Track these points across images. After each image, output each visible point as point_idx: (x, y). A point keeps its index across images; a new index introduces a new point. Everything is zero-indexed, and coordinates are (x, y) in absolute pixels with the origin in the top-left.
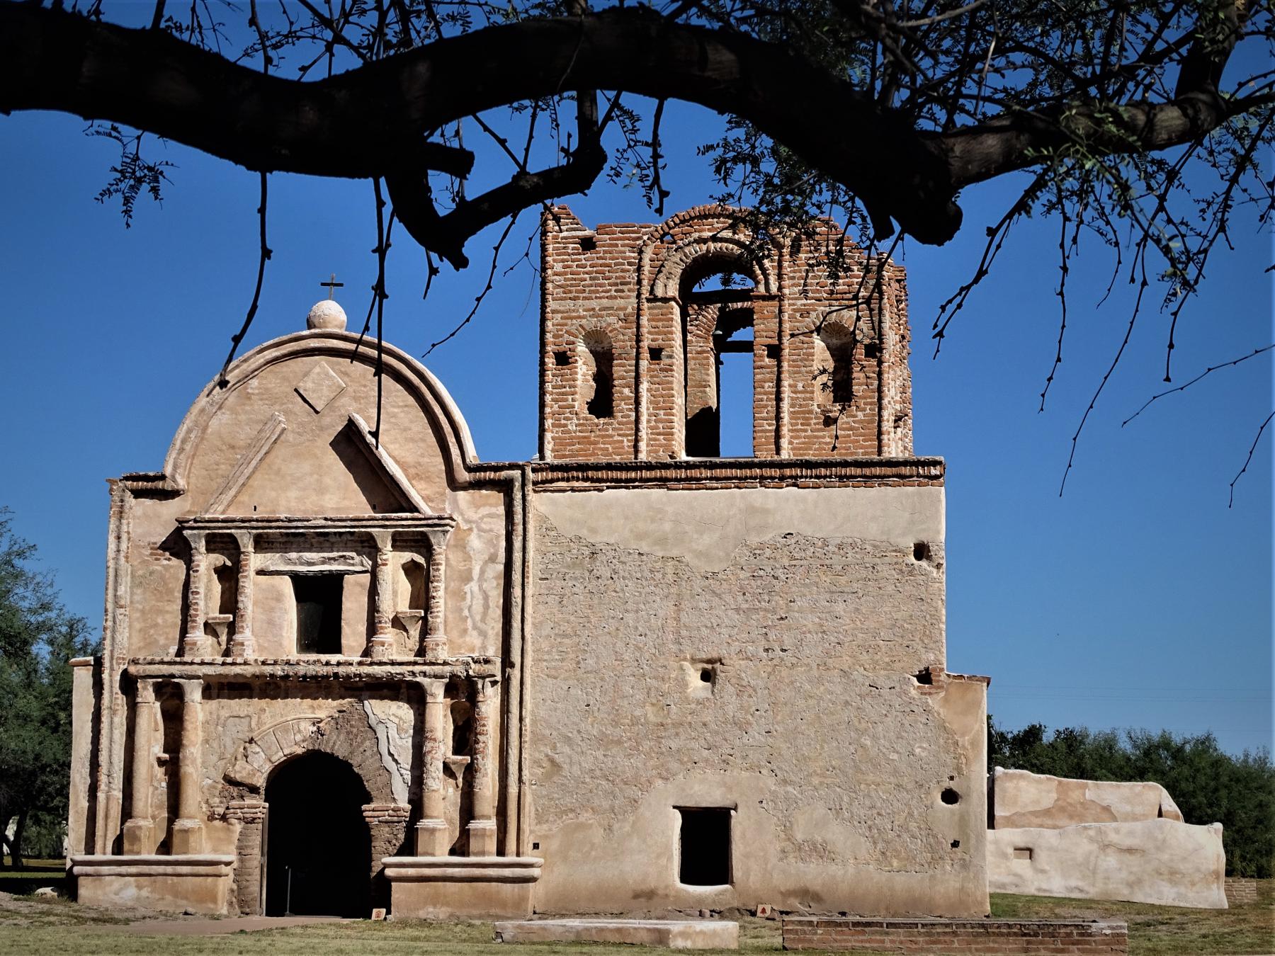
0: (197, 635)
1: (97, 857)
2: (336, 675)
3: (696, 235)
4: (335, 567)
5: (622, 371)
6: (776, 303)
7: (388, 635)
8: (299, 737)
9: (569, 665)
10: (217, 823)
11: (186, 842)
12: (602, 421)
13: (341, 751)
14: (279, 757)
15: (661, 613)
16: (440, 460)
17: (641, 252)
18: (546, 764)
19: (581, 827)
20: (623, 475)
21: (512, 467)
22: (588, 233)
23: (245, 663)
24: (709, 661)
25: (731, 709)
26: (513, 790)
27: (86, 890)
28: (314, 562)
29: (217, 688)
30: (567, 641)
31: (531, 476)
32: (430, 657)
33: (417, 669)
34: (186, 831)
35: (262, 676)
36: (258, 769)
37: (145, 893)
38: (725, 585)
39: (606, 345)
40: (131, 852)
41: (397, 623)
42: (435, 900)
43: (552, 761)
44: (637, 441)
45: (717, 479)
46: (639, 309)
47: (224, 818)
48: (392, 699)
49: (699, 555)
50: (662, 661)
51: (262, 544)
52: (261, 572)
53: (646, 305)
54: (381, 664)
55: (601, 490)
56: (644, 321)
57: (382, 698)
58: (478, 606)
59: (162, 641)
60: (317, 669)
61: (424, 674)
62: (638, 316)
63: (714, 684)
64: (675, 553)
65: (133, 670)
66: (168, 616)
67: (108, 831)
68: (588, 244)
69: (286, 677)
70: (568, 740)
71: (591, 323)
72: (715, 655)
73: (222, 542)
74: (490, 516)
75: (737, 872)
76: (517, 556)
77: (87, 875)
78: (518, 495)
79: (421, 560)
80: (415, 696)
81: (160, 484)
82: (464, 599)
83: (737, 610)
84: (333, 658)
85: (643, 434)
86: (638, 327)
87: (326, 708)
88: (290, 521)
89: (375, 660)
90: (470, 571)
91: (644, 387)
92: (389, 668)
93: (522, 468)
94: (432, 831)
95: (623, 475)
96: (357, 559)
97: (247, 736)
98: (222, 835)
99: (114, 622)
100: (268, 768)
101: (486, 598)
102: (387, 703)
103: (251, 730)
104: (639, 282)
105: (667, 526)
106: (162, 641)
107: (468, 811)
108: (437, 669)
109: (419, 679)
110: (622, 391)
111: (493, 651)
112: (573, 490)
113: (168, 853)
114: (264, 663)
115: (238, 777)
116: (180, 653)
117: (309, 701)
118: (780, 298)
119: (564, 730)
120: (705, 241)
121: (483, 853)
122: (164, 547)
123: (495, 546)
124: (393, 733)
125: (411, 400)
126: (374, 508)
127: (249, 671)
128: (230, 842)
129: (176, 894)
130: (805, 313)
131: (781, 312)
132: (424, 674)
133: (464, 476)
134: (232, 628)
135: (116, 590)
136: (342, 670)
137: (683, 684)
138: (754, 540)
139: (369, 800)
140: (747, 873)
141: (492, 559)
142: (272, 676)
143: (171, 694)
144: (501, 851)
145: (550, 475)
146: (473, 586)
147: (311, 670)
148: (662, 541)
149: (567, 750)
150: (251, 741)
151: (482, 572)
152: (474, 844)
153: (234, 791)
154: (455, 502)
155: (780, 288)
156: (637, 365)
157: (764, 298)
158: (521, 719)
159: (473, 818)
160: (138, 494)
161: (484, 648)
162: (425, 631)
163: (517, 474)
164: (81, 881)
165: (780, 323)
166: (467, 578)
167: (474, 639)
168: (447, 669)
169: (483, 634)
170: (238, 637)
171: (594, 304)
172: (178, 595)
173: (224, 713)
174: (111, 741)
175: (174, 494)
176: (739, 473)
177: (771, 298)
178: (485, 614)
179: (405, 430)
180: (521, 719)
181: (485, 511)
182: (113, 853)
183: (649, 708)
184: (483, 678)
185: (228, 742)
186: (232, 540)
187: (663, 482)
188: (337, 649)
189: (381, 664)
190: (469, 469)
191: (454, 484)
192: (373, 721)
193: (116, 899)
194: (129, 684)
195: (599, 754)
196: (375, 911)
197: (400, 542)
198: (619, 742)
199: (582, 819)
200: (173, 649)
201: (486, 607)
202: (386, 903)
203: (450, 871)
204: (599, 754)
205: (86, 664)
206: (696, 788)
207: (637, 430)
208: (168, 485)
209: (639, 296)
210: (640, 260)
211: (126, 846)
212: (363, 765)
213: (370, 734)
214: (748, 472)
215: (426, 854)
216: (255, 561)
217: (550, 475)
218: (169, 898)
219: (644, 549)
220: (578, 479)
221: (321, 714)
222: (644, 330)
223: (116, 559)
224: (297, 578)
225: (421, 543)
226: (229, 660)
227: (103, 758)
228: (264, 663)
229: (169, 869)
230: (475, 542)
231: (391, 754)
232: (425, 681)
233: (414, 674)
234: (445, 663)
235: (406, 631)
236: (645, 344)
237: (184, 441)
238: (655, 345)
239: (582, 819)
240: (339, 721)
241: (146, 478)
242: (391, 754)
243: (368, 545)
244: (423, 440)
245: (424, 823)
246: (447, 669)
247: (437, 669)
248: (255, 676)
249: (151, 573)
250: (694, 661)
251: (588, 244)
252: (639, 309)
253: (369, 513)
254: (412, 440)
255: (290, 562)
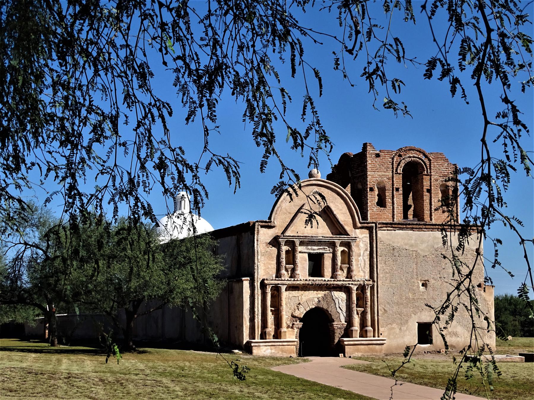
0: (283, 271)
1: (256, 340)
2: (327, 284)
3: (408, 155)
4: (321, 251)
5: (388, 194)
6: (429, 177)
7: (339, 272)
8: (314, 303)
9: (388, 281)
10: (290, 329)
11: (285, 335)
12: (382, 208)
13: (325, 307)
14: (308, 309)
15: (412, 267)
16: (351, 220)
17: (393, 159)
18: (383, 310)
19: (394, 328)
20: (402, 226)
21: (373, 223)
22: (378, 152)
23: (301, 280)
24: (425, 281)
25: (431, 294)
26: (376, 318)
27: (255, 351)
28: (315, 249)
29: (292, 288)
30: (388, 275)
31: (378, 226)
32: (353, 279)
33: (350, 282)
34: (285, 332)
35: (306, 284)
36: (301, 313)
37: (273, 351)
38: (429, 259)
39: (381, 186)
40: (269, 339)
41: (341, 269)
42: (358, 351)
43: (384, 310)
44: (393, 215)
45: (427, 229)
46: (393, 176)
47: (292, 328)
48: (340, 291)
49: (422, 250)
50: (413, 280)
51: (302, 243)
52: (300, 252)
53: (395, 175)
54: (340, 281)
55: (395, 230)
56: (394, 180)
57: (337, 291)
58: (363, 264)
59: (271, 273)
60: (322, 282)
61: (352, 284)
62: (393, 178)
63: (426, 287)
64: (415, 249)
65: (266, 282)
66: (272, 265)
67: (258, 332)
68: (378, 156)
69: (312, 285)
70: (388, 303)
71: (379, 179)
72: (426, 279)
73: (291, 243)
74: (365, 237)
75: (434, 341)
76: (375, 249)
77: (256, 346)
78: (374, 231)
79: (346, 250)
80: (347, 290)
81: (270, 224)
82: (359, 261)
83: (432, 266)
84: (323, 279)
85: (395, 213)
86: (393, 181)
87: (321, 294)
88: (312, 237)
89: (339, 279)
90: (360, 253)
91: (395, 199)
92: (342, 282)
93: (376, 223)
94: (357, 331)
95: (402, 226)
96: (328, 249)
97: (298, 302)
98: (291, 333)
99: (258, 267)
100: (305, 312)
101: (365, 261)
102: (338, 292)
103: (299, 300)
104: (393, 168)
105: (413, 242)
106: (271, 273)
107: (363, 325)
108: (356, 283)
109: (350, 285)
110: (389, 200)
111: (367, 277)
112: (388, 230)
113: (277, 338)
114: (306, 280)
115: (296, 315)
116: (276, 277)
117: (315, 292)
118: (431, 176)
119: (388, 301)
120: (410, 157)
121: (371, 337)
122: (270, 243)
123: (367, 246)
124: (340, 302)
125: (342, 201)
126: (332, 233)
127: (302, 283)
128: (293, 335)
129: (283, 351)
130: (437, 180)
131: (431, 179)
132: (352, 284)
133: (359, 225)
134: (293, 270)
135: (258, 257)
136: (329, 283)
137: (418, 287)
138: (436, 246)
139: (334, 321)
140: (437, 341)
141: (366, 250)
142: (308, 284)
143: (276, 289)
144: (374, 336)
145: (382, 226)
146: (361, 257)
147: (320, 283)
148: (412, 246)
149: (388, 306)
150: (299, 304)
151: (364, 254)
152: (368, 334)
153: (294, 319)
154: (355, 233)
155: (430, 172)
156: (393, 193)
157: (426, 175)
158: (377, 297)
159: (367, 326)
160: (262, 227)
161: (365, 276)
162: (350, 270)
163: (374, 225)
164: (254, 348)
165: (431, 183)
166: (360, 256)
167: (362, 273)
168: (359, 283)
169: (364, 272)
170: (297, 272)
171: (380, 173)
172: (275, 259)
173: (291, 295)
174: (258, 304)
175: (274, 227)
176: (432, 227)
177: (428, 175)
178: (364, 267)
179: (341, 210)
180: (377, 297)
181: (364, 235)
182: (273, 339)
183: (410, 294)
184: (368, 285)
185: (292, 304)
186: (293, 242)
187: (412, 229)
188: (322, 275)
189: (340, 281)
190: (361, 223)
191: (355, 227)
192: (334, 298)
193: (265, 353)
194: (263, 285)
195: (397, 307)
196: (340, 355)
197: (342, 244)
198: (403, 304)
199: (393, 326)
200: (274, 276)
201: (365, 264)
202: (344, 352)
203: (363, 342)
204: (397, 307)
205: (247, 280)
206: (423, 317)
207: (393, 212)
208: (272, 224)
209: (393, 172)
210: (393, 161)
211: (267, 337)
212: (331, 310)
213: (333, 302)
214: (434, 227)
215: (355, 337)
216: (300, 248)
217: (382, 226)
218: (280, 352)
219: (407, 248)
220: (389, 227)
221: (320, 296)
222: (395, 182)
223: (257, 247)
224: (310, 255)
225: (348, 245)
226: (296, 279)
227: (256, 310)
228: (306, 280)
229: (281, 344)
230: (361, 245)
231: (339, 307)
232: (352, 286)
233: (349, 284)
234: (358, 281)
235: (343, 271)
236: (395, 186)
237: (276, 211)
238: (397, 187)
239: (393, 326)
240: (325, 298)
241: (266, 222)
242: (339, 307)
243: (332, 245)
244: (346, 214)
245: (353, 328)
246: (359, 283)
247: (356, 283)
248: (303, 284)
249: (267, 252)
250: (421, 280)
251: (378, 156)
252: (393, 176)
253: (331, 236)
254: (343, 214)
255: (308, 249)
